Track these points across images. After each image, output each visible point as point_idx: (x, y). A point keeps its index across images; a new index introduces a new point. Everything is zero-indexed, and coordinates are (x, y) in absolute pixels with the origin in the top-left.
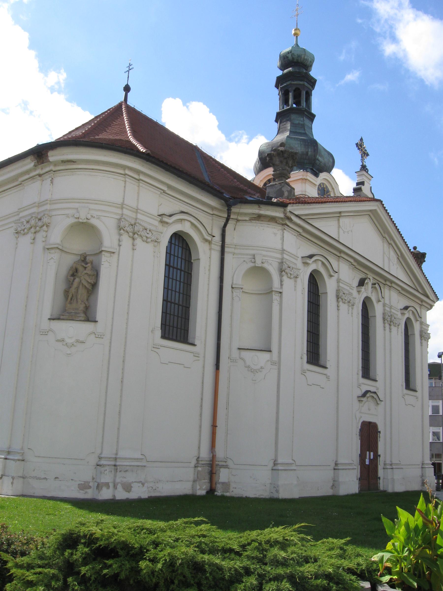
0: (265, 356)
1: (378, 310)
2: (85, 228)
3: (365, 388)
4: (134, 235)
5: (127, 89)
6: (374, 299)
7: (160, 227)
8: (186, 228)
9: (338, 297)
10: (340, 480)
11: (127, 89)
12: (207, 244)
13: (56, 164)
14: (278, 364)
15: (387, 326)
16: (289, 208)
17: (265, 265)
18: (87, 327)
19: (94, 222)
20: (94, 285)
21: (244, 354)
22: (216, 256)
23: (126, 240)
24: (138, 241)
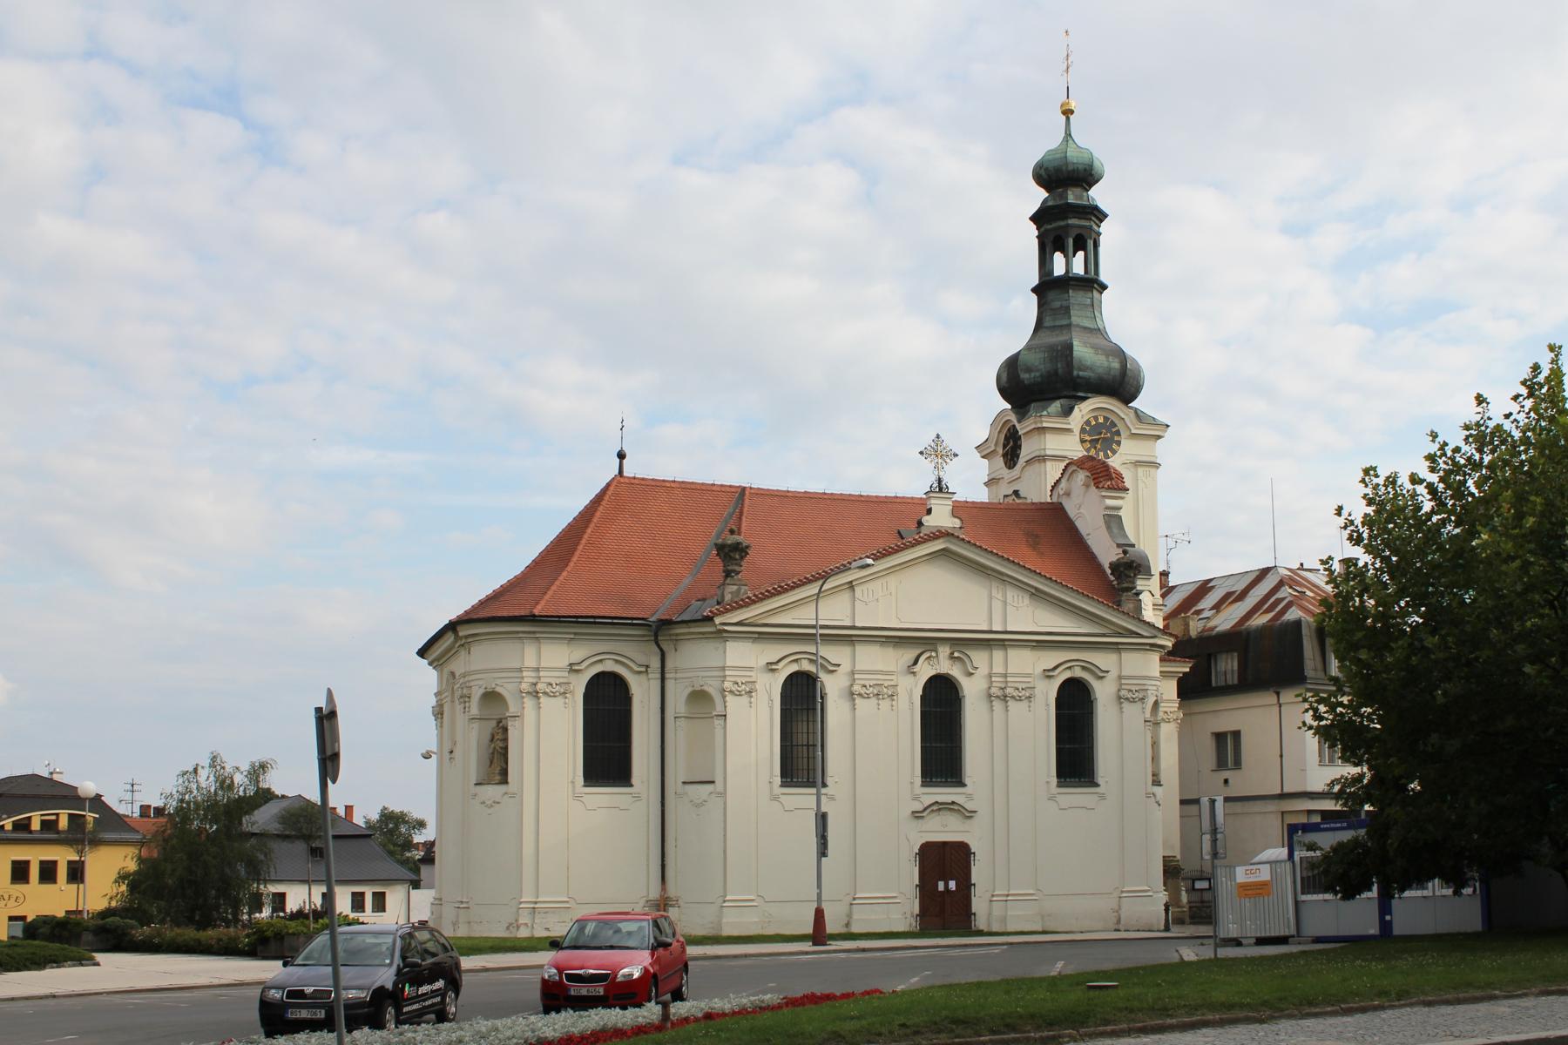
0: (709, 787)
1: (972, 689)
2: (491, 697)
3: (928, 800)
4: (535, 694)
5: (621, 456)
6: (955, 672)
7: (573, 678)
8: (609, 666)
9: (852, 695)
10: (855, 917)
11: (621, 456)
12: (643, 677)
13: (467, 637)
14: (723, 794)
15: (998, 705)
16: (718, 620)
17: (706, 688)
18: (503, 788)
19: (498, 689)
20: (506, 748)
21: (688, 787)
22: (655, 685)
23: (529, 703)
24: (543, 699)
